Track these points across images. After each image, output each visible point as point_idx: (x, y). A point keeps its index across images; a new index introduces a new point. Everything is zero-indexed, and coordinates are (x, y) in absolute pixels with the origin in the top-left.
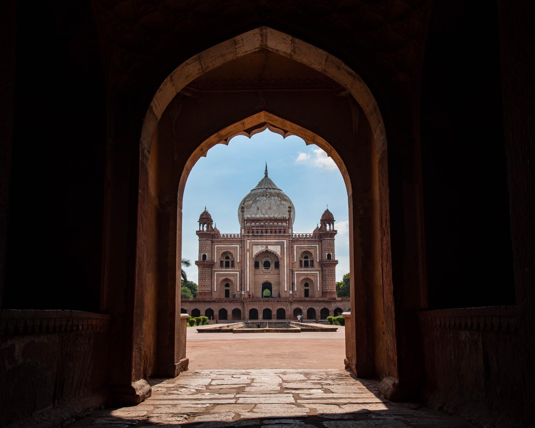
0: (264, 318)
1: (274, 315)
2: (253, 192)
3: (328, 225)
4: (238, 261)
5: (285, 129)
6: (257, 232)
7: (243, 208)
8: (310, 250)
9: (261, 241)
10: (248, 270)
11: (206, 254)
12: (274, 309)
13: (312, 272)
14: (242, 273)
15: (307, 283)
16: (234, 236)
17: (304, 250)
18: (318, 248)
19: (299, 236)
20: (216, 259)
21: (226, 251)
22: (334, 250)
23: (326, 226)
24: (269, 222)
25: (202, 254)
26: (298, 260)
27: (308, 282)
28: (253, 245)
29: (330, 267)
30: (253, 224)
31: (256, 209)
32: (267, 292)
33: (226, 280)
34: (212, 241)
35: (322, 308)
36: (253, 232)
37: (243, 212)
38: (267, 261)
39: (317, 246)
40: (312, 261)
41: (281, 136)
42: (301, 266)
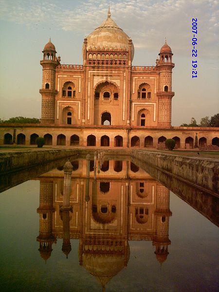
0: (102, 145)
1: (112, 142)
3: (166, 59)
4: (80, 91)
6: (99, 63)
11: (49, 83)
20: (59, 88)
22: (171, 83)
25: (46, 83)
26: (137, 91)
27: (144, 112)
28: (94, 75)
32: (107, 123)
37: (86, 43)
40: (149, 93)
42: (139, 97)
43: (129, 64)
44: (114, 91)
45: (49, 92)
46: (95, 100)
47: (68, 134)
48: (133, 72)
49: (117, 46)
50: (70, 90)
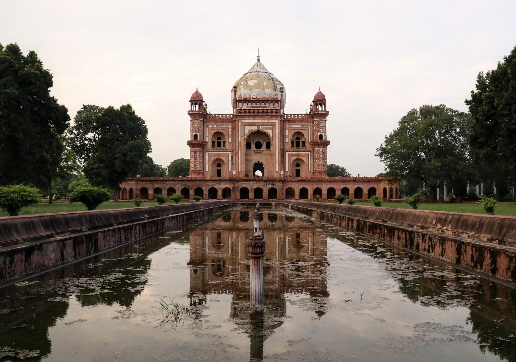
0: (256, 197)
3: (320, 106)
4: (230, 142)
7: (235, 87)
8: (301, 131)
11: (198, 134)
12: (266, 188)
15: (298, 163)
18: (309, 128)
20: (209, 139)
25: (194, 134)
27: (300, 163)
33: (218, 159)
34: (204, 121)
40: (304, 143)
42: (292, 146)
43: (282, 113)
44: (265, 141)
45: (196, 144)
47: (220, 187)
48: (287, 121)
49: (268, 93)
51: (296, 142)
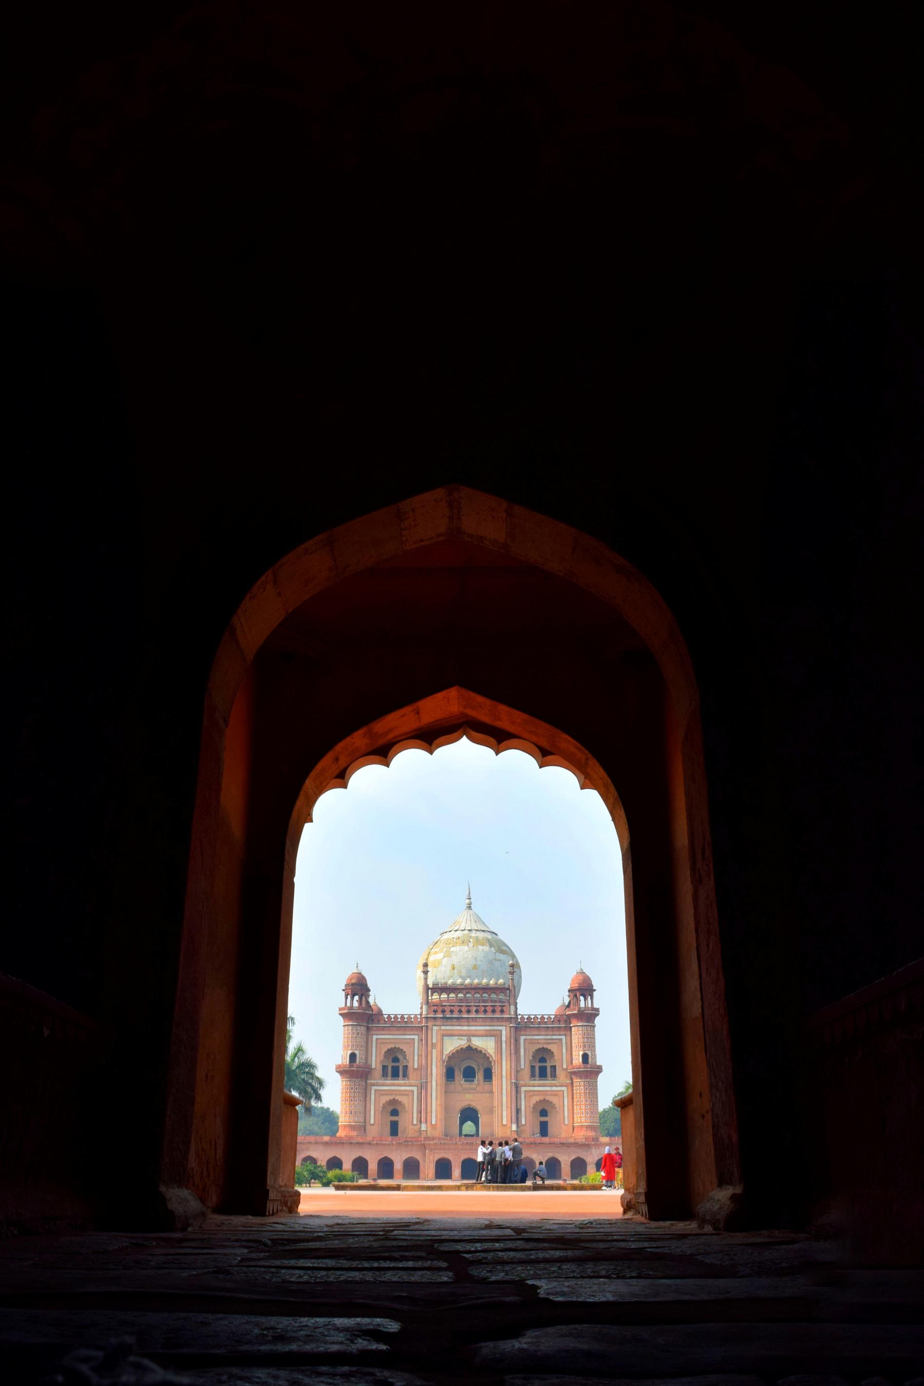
0: (464, 1176)
2: (446, 936)
3: (582, 998)
4: (416, 1066)
5: (500, 724)
6: (452, 1011)
7: (426, 965)
8: (549, 1047)
9: (458, 1028)
10: (434, 1083)
11: (357, 1052)
13: (554, 1088)
14: (423, 1087)
16: (409, 1018)
17: (538, 1046)
19: (529, 1018)
20: (375, 1062)
21: (393, 1046)
22: (594, 1047)
23: (578, 1001)
24: (473, 992)
25: (349, 1052)
26: (528, 1064)
28: (444, 1035)
29: (586, 1077)
30: (444, 996)
31: (450, 968)
32: (469, 1127)
33: (394, 1102)
34: (368, 1028)
35: (573, 1157)
36: (443, 1011)
37: (426, 973)
38: (468, 1067)
39: (563, 1037)
40: (554, 1068)
41: (489, 752)
42: (533, 1075)
46: (446, 1084)
48: (522, 1026)
50: (397, 1064)
51: (540, 1067)
